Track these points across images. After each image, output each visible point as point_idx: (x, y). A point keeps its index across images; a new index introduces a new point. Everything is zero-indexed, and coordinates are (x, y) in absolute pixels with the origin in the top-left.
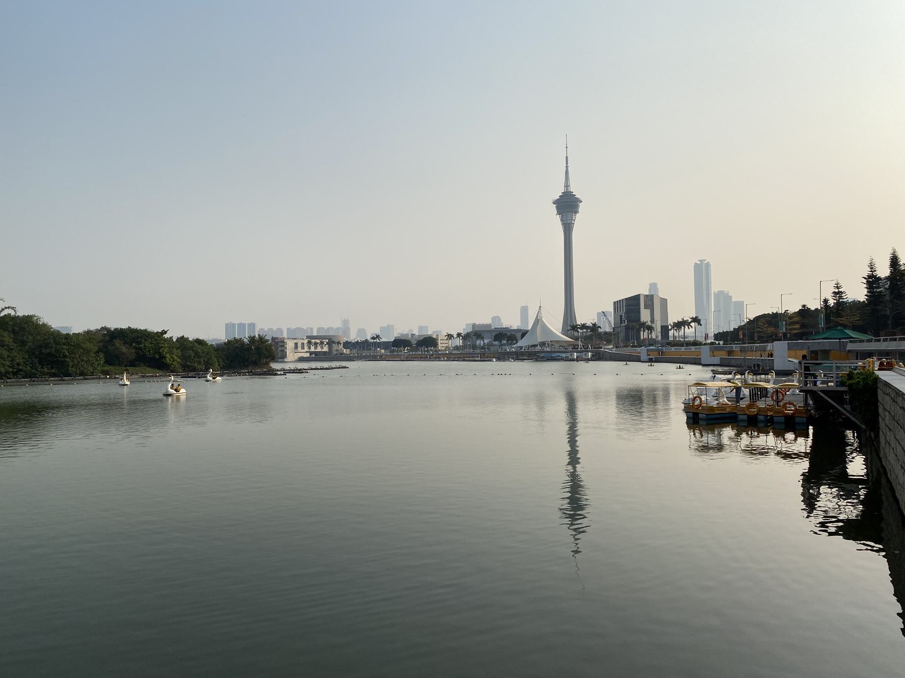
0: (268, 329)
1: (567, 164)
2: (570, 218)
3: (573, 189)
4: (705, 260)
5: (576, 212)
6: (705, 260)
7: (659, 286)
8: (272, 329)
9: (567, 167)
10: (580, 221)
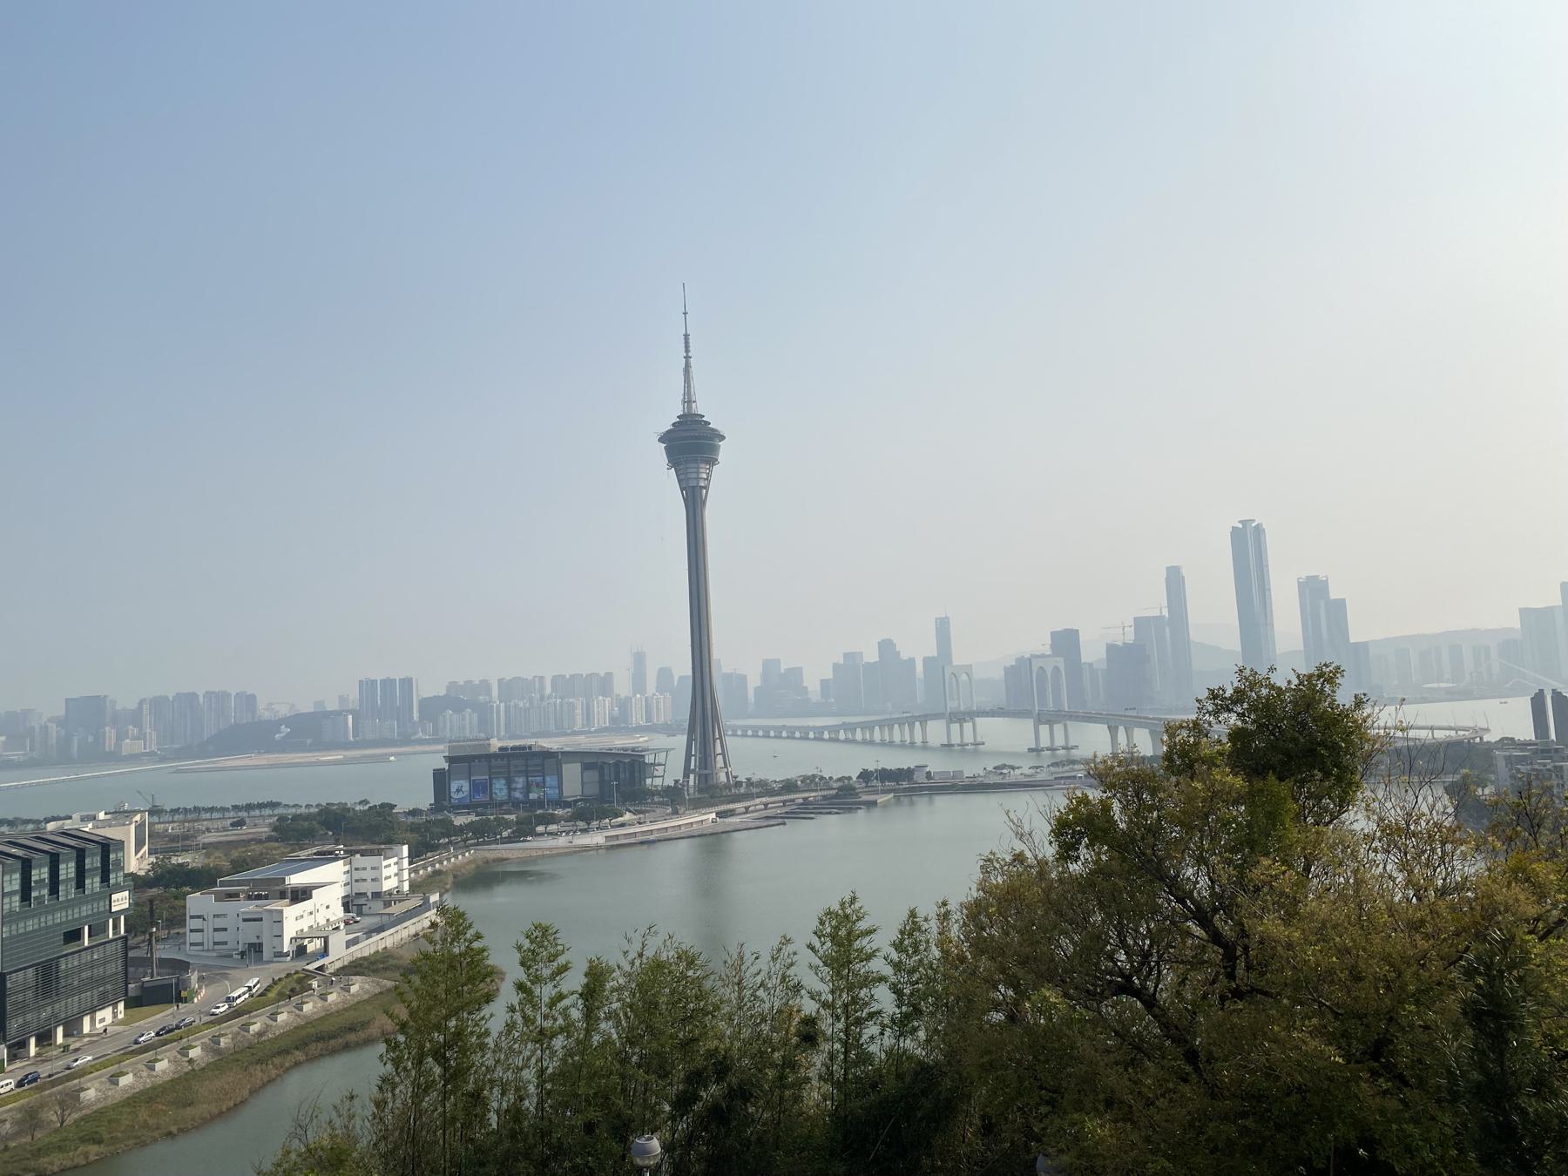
0: (480, 681)
1: (687, 350)
2: (694, 476)
3: (700, 408)
4: (1254, 521)
5: (713, 462)
6: (1254, 521)
7: (1184, 572)
8: (471, 681)
9: (687, 358)
10: (721, 480)
